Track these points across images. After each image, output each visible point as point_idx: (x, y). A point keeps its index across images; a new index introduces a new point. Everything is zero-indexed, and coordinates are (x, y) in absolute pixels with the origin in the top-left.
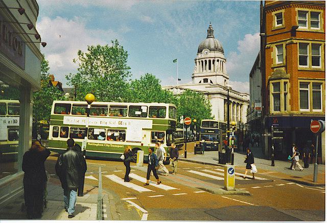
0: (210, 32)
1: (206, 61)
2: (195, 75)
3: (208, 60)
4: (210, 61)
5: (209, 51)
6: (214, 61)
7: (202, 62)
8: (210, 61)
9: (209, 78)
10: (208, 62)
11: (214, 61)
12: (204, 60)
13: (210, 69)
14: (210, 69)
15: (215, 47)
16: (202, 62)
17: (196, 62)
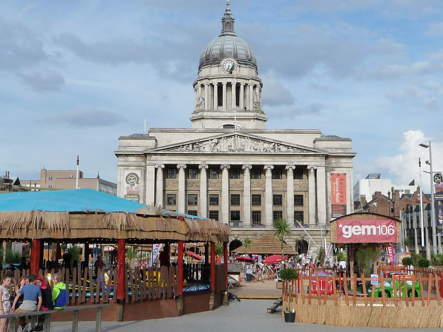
0: (228, 23)
1: (229, 85)
2: (205, 114)
3: (234, 82)
4: (238, 86)
5: (236, 63)
6: (246, 86)
7: (220, 86)
8: (238, 86)
9: (238, 124)
10: (234, 87)
11: (246, 86)
12: (224, 82)
13: (238, 104)
14: (238, 104)
15: (247, 56)
16: (220, 86)
17: (202, 86)
